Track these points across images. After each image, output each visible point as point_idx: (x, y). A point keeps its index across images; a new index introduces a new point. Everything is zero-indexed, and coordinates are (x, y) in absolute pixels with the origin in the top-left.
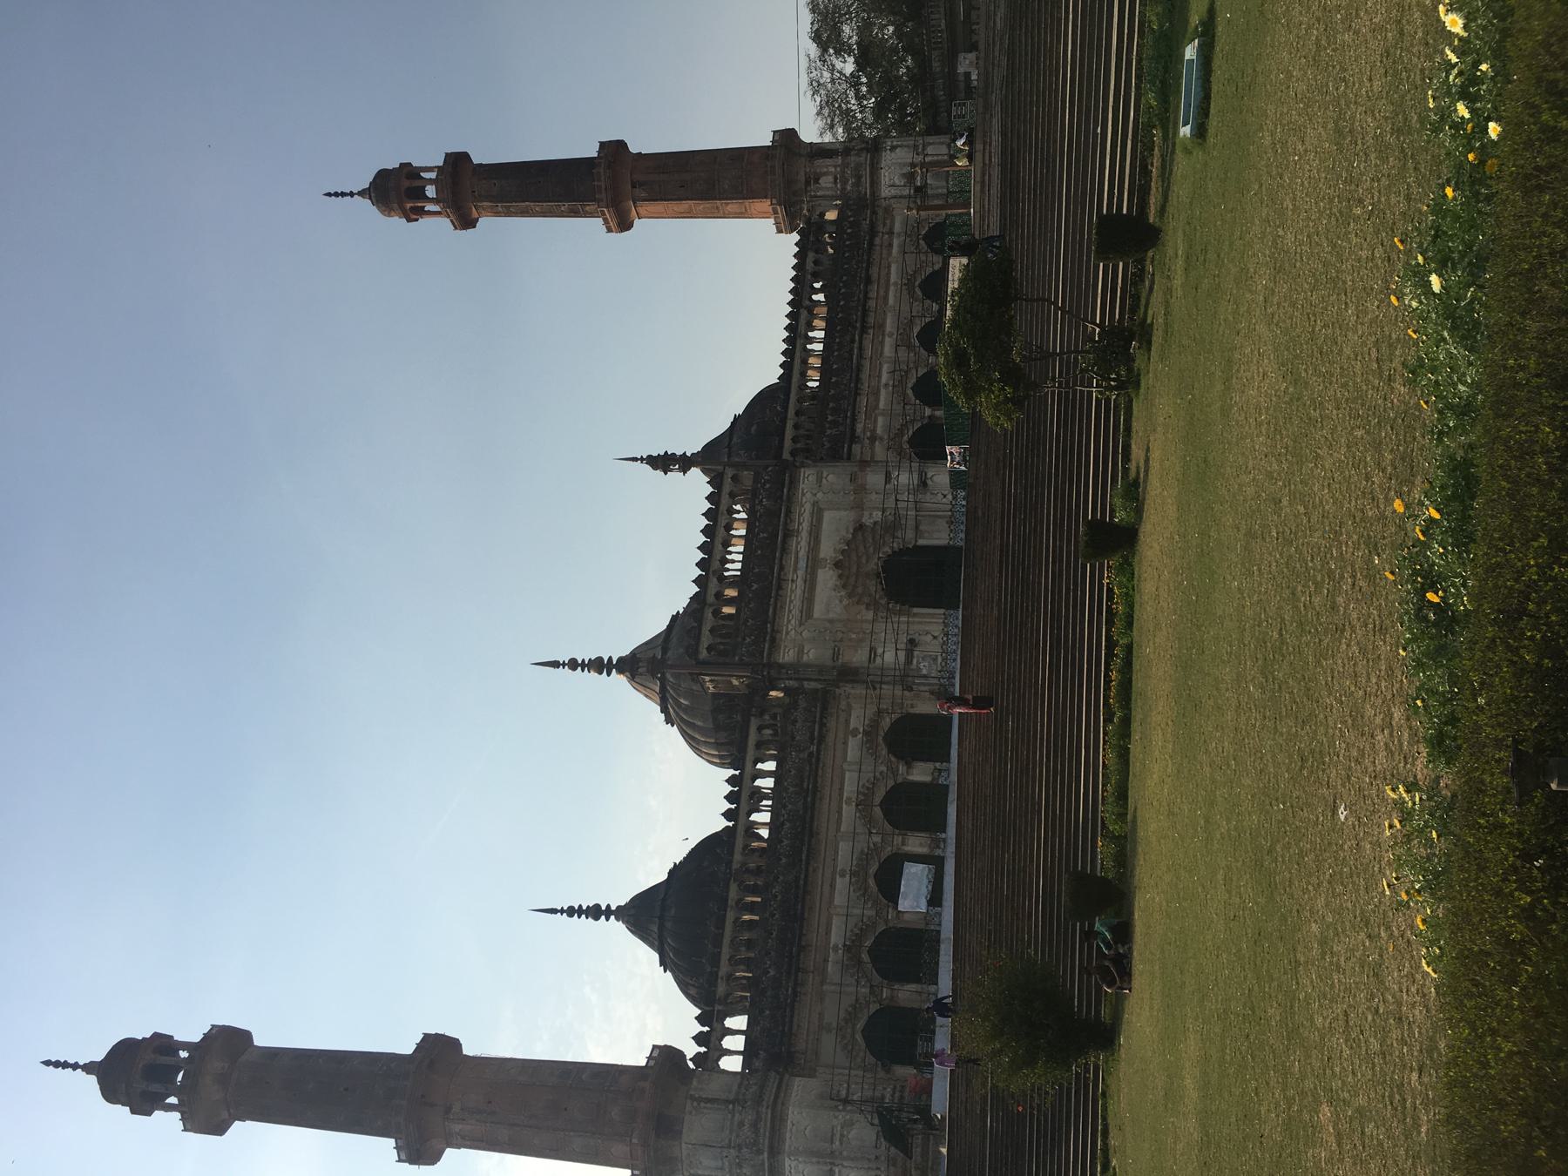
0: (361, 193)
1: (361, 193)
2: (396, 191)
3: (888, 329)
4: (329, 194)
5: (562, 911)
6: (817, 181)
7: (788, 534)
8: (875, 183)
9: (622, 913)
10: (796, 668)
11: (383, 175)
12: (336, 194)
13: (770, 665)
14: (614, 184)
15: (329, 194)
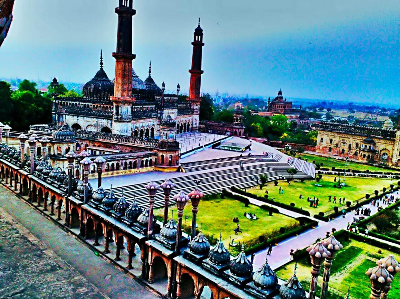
0: (199, 26)
1: (199, 26)
2: (199, 32)
3: (183, 118)
4: (199, 19)
5: (101, 56)
6: (197, 106)
7: (173, 109)
8: (195, 114)
9: (102, 69)
10: (162, 114)
11: (202, 30)
12: (199, 20)
13: (164, 109)
14: (196, 71)
15: (199, 19)
